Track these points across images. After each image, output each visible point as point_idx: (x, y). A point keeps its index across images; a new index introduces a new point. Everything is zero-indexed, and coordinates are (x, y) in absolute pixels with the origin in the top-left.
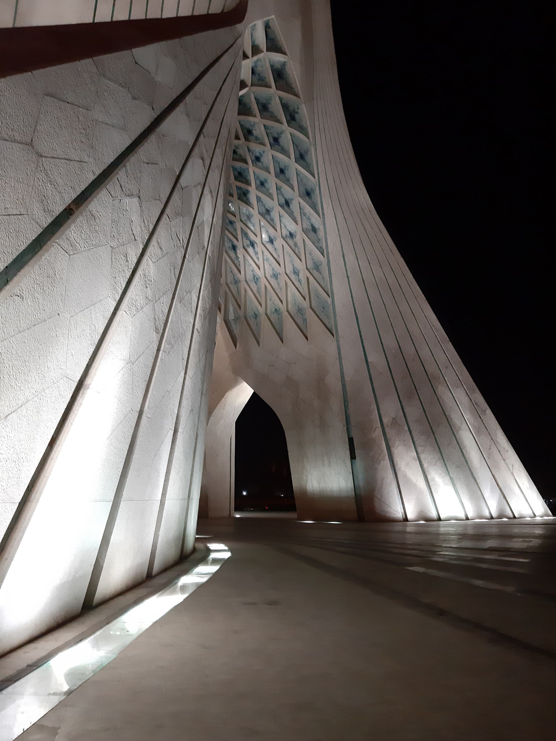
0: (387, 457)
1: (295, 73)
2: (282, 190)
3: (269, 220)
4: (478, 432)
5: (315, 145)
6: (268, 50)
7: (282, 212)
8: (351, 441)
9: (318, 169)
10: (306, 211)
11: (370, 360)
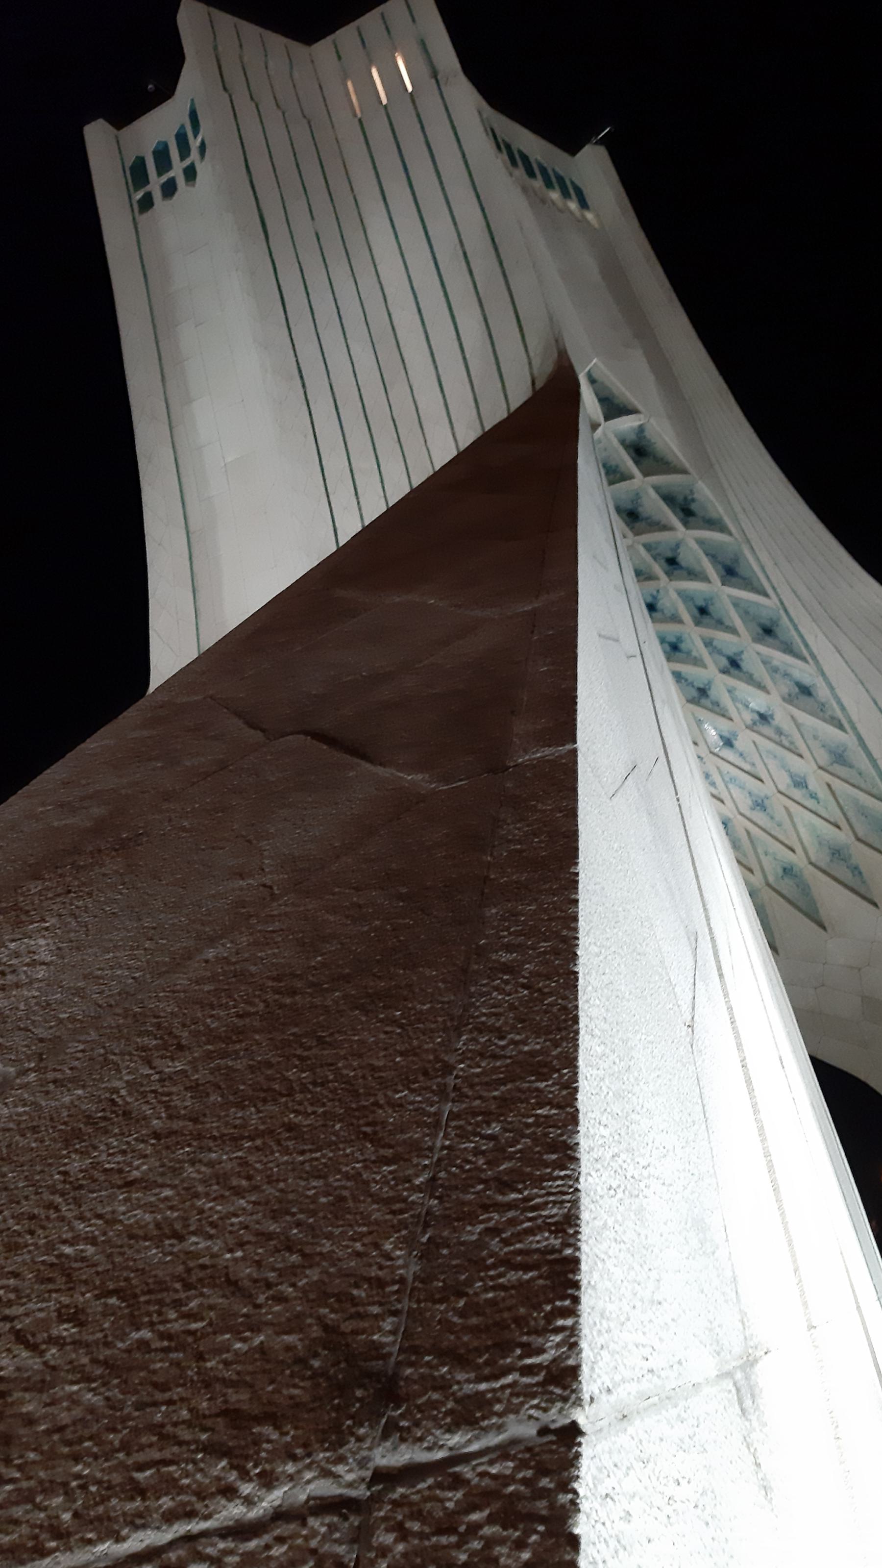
1: (665, 437)
2: (715, 643)
5: (748, 541)
6: (607, 418)
9: (768, 577)
10: (775, 663)
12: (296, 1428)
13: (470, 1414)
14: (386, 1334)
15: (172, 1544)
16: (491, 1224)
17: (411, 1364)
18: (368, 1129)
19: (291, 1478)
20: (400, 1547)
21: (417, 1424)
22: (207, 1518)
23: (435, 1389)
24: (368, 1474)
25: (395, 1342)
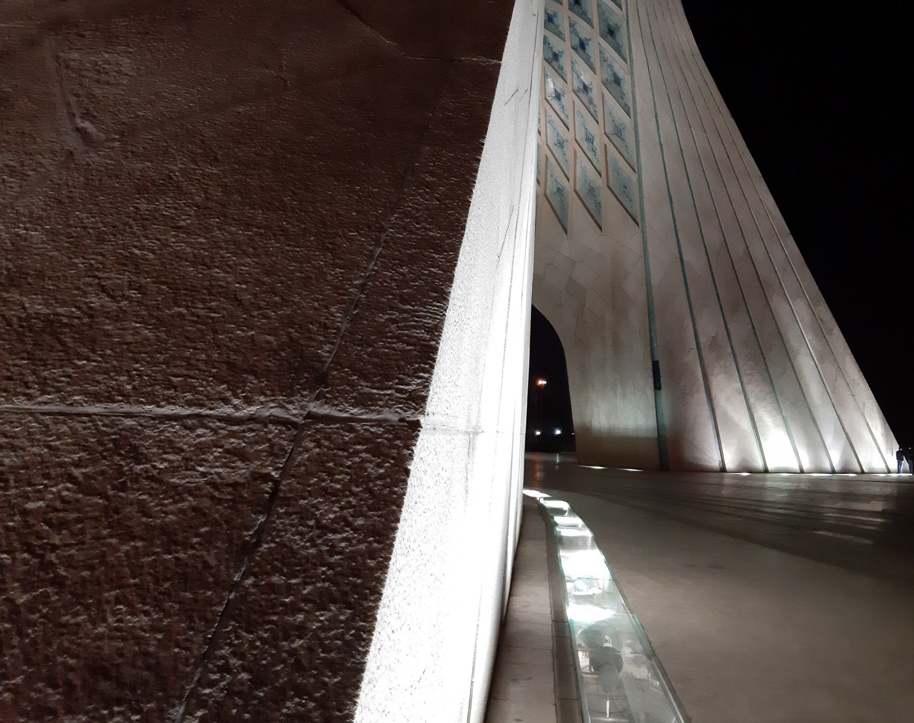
0: (703, 388)
3: (556, 67)
4: (822, 358)
7: (576, 57)
8: (655, 366)
10: (607, 55)
11: (685, 258)
12: (268, 381)
13: (364, 401)
14: (325, 352)
15: (189, 416)
16: (393, 317)
17: (337, 370)
18: (330, 246)
19: (262, 403)
20: (317, 450)
21: (336, 398)
22: (211, 409)
23: (348, 385)
24: (305, 413)
25: (329, 357)
